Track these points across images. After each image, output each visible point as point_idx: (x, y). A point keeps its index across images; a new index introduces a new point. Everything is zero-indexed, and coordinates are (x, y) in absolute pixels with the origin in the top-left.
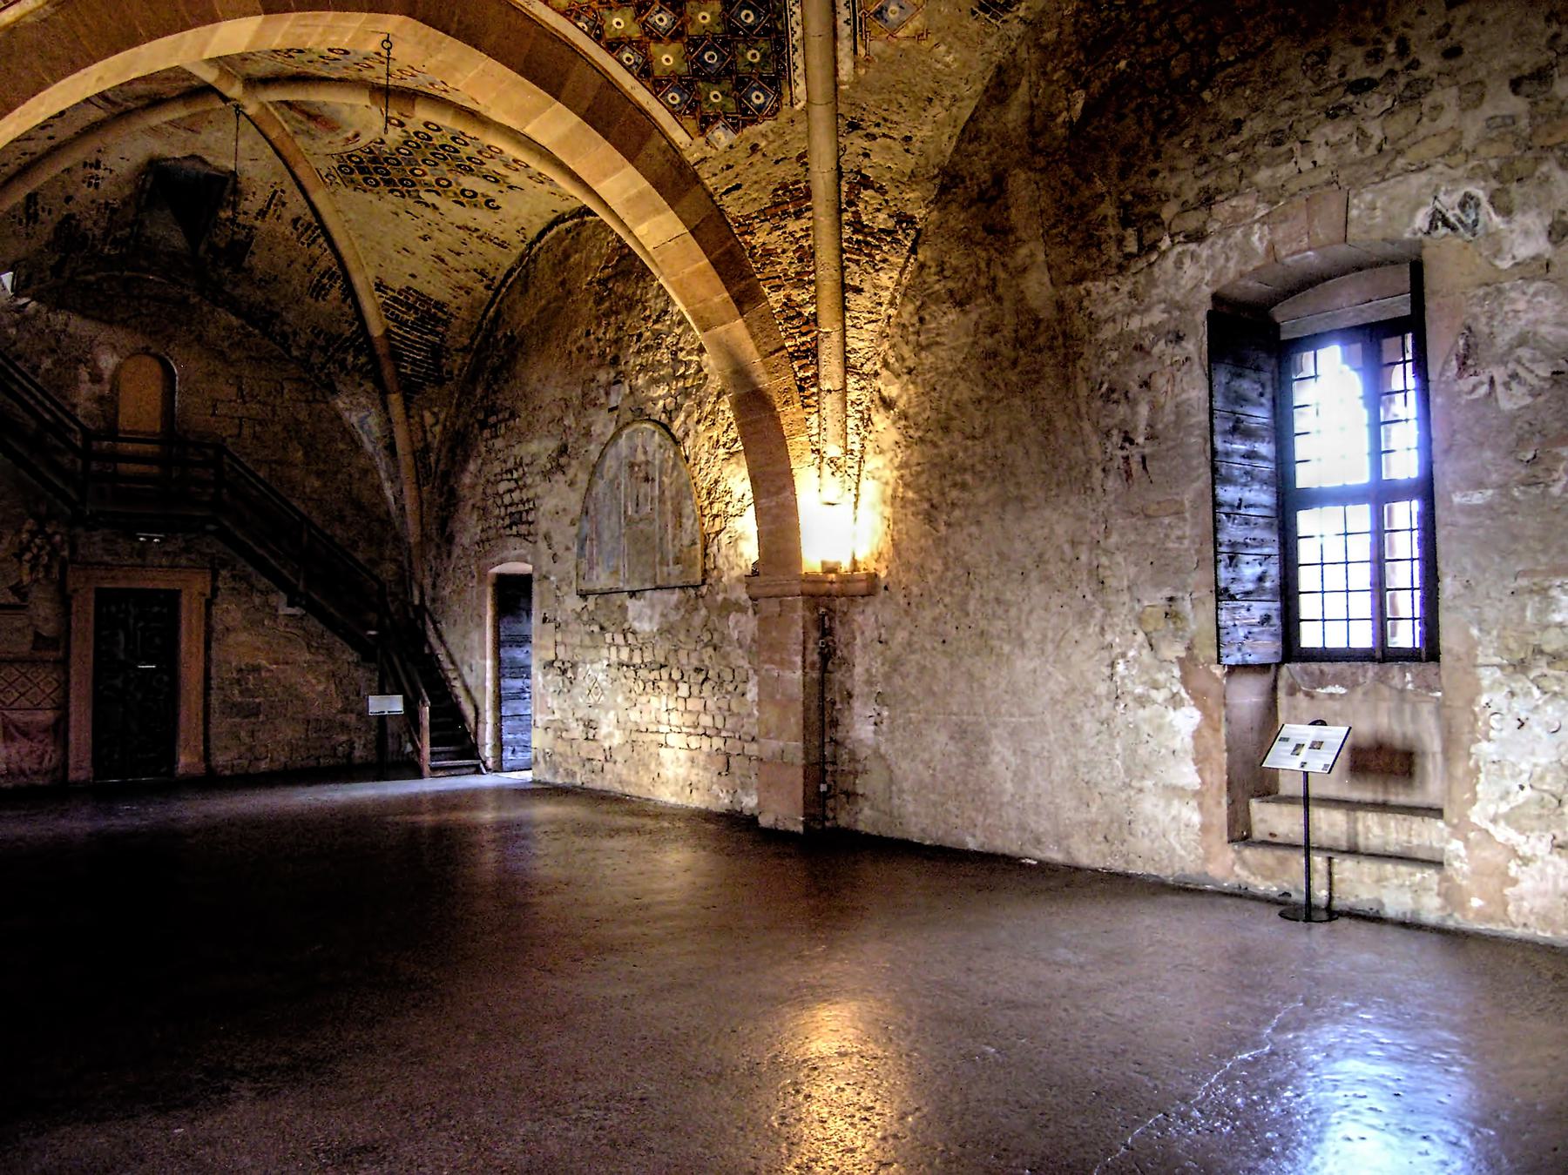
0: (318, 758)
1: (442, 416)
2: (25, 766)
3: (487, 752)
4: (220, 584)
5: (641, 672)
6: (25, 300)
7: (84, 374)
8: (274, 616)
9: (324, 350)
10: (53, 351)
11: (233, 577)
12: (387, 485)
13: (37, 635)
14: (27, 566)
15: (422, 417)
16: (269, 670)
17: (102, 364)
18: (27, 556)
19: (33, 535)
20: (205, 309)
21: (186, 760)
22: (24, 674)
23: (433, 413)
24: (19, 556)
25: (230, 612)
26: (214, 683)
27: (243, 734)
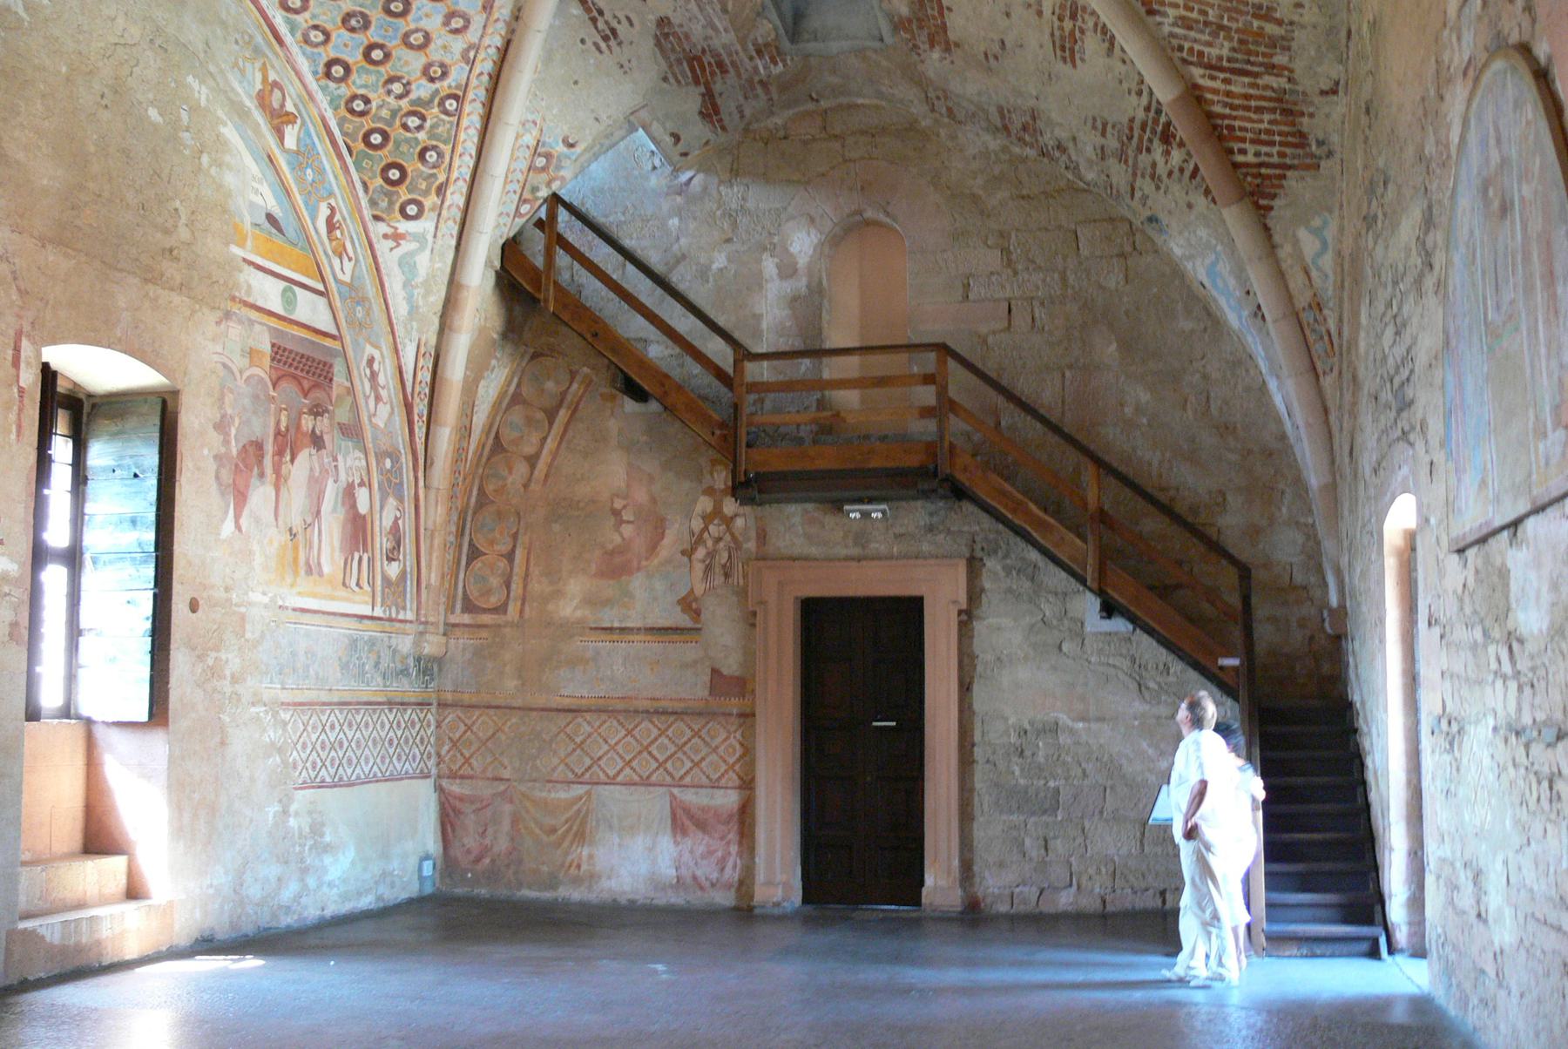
0: (1163, 893)
1: (1330, 234)
2: (699, 873)
3: (1397, 911)
4: (987, 585)
5: (1536, 749)
6: (689, 174)
7: (769, 266)
8: (1079, 635)
9: (1122, 157)
10: (729, 241)
11: (1008, 570)
12: (1273, 385)
13: (715, 672)
14: (699, 568)
15: (1296, 242)
16: (1072, 731)
17: (795, 248)
18: (701, 553)
19: (707, 519)
20: (943, 132)
21: (939, 884)
22: (697, 734)
23: (1317, 232)
24: (688, 553)
25: (1004, 630)
26: (978, 752)
27: (1028, 842)
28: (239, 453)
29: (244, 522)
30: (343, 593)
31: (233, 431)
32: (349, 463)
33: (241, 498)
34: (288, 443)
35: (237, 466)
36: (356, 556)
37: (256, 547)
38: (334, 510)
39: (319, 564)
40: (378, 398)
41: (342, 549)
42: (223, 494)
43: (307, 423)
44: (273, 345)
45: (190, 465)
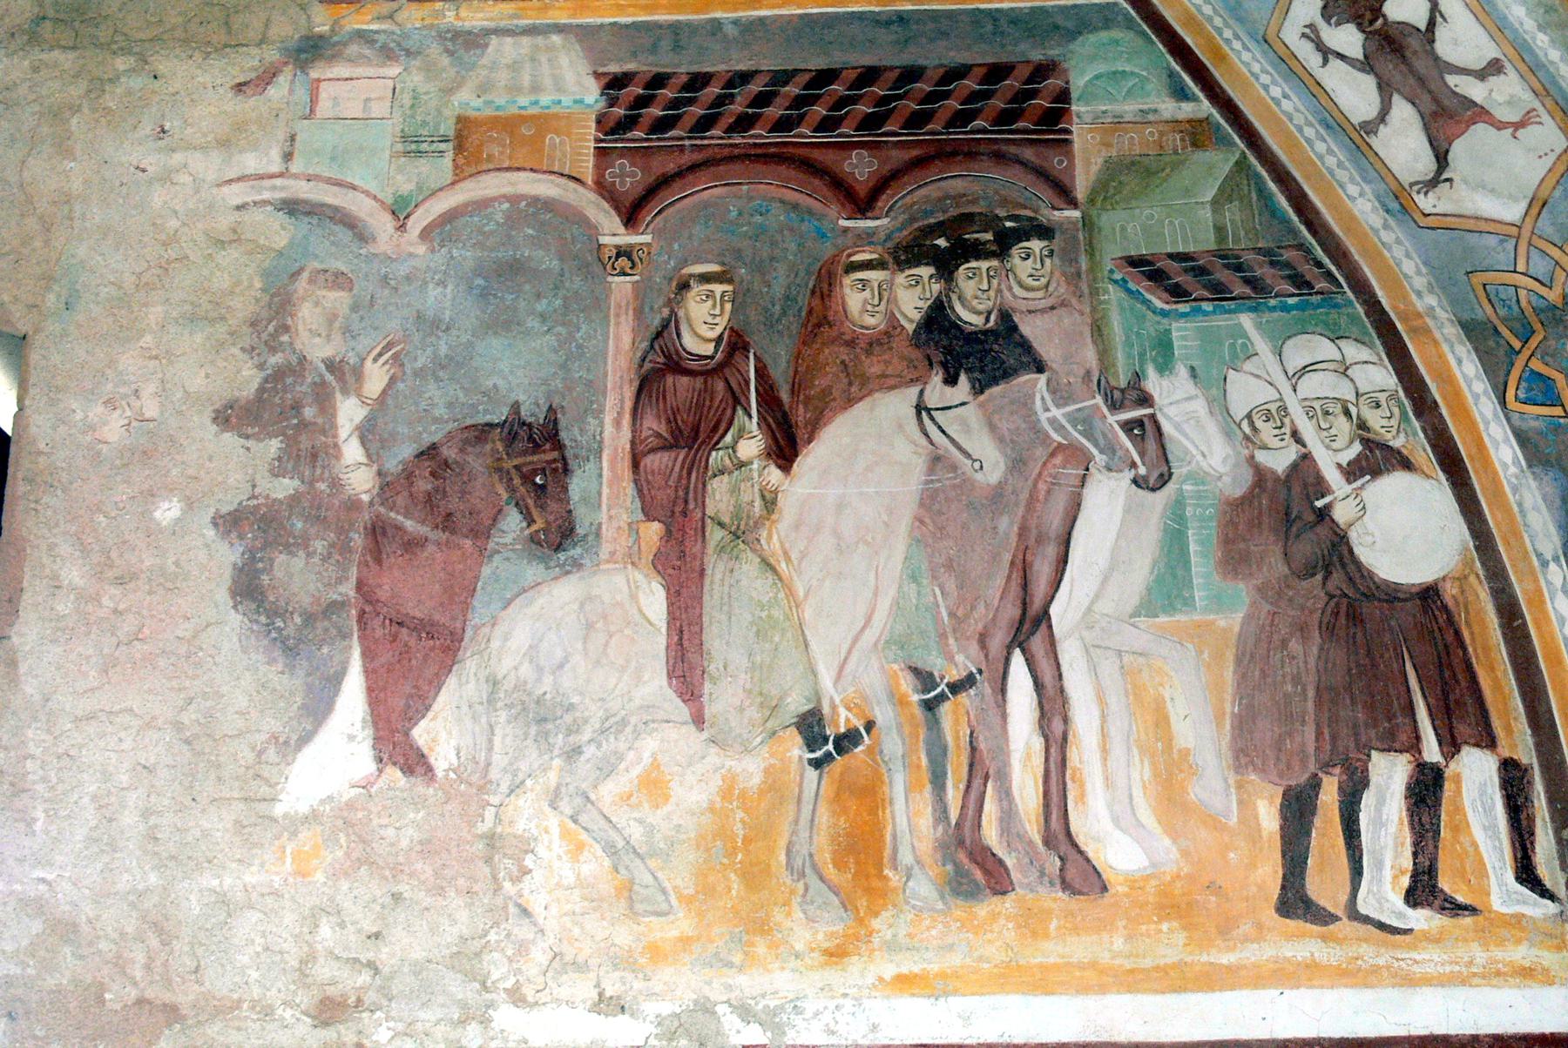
28: (387, 487)
29: (441, 732)
30: (1301, 944)
31: (350, 413)
32: (1246, 392)
33: (413, 653)
34: (729, 403)
35: (378, 532)
36: (1390, 776)
37: (527, 814)
38: (1168, 590)
39: (1059, 834)
40: (1446, 119)
41: (1244, 755)
42: (290, 649)
43: (893, 298)
44: (614, 84)
45: (73, 574)
